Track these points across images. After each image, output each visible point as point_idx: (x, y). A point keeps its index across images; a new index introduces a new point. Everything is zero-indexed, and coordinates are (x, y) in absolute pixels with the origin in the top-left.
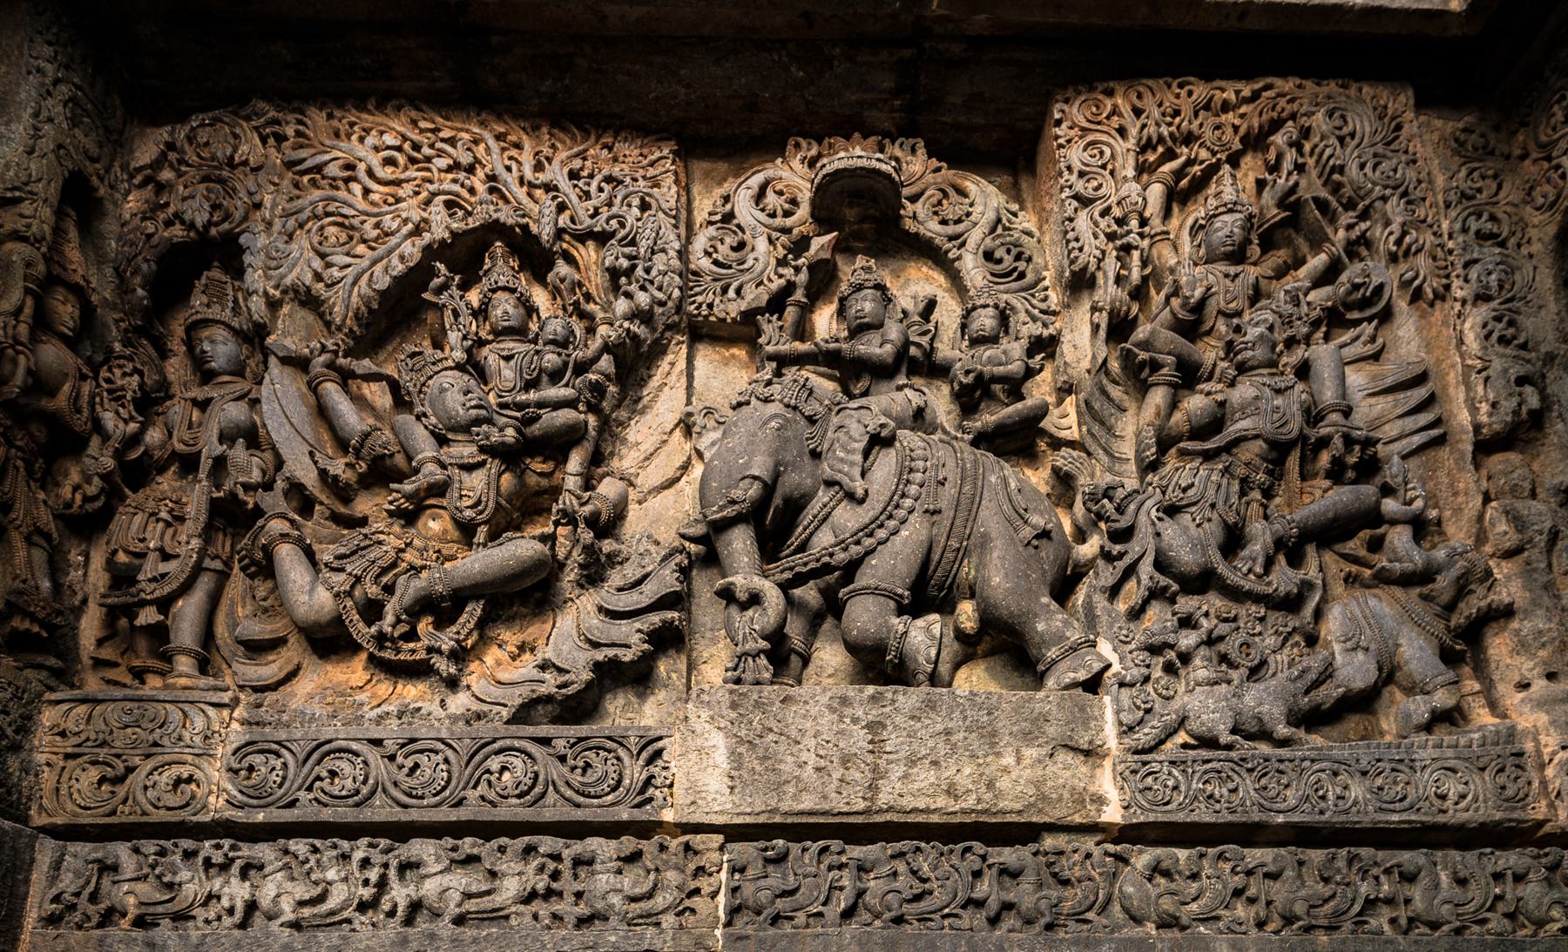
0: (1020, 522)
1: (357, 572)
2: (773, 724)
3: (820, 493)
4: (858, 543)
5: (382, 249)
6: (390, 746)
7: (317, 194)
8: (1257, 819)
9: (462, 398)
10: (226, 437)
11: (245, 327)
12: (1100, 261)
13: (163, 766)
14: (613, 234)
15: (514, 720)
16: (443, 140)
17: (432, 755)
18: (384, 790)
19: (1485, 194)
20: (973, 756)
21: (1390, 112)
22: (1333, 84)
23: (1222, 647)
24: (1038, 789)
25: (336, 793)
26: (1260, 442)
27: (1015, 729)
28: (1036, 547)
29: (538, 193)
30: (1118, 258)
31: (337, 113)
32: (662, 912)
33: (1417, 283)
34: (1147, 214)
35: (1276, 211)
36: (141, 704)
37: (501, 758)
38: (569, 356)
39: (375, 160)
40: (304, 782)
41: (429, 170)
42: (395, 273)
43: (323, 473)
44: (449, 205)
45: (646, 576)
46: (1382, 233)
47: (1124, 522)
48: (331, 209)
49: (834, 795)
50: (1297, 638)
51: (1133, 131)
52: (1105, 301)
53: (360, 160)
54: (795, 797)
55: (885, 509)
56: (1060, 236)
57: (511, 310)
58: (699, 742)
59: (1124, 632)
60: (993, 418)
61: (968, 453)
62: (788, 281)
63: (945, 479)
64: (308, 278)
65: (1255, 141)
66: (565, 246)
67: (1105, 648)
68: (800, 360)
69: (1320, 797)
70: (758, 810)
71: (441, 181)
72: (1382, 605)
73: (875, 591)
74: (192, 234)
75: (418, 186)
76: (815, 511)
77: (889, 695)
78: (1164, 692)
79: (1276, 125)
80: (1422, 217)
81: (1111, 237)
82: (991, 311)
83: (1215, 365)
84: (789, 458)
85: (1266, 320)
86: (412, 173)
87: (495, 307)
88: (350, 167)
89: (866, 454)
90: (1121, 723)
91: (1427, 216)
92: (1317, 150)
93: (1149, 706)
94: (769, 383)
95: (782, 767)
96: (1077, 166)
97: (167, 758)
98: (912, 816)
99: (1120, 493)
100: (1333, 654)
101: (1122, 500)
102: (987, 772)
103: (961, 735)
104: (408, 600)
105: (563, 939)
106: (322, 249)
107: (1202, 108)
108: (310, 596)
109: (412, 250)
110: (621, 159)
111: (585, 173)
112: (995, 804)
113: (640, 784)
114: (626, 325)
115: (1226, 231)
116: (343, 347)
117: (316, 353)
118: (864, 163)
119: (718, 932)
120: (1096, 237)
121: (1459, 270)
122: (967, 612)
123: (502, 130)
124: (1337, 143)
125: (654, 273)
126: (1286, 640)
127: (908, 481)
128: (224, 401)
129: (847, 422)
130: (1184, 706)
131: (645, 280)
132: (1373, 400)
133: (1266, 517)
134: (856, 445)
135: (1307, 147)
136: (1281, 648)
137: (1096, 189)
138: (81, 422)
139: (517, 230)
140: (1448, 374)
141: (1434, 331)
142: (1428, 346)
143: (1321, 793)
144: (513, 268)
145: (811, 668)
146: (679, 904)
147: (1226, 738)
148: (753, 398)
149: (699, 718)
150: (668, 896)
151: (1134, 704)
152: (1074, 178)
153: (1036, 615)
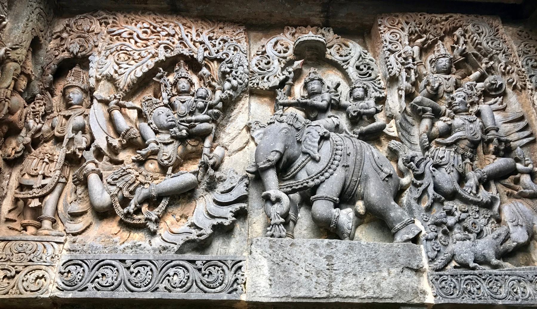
0: (380, 171)
1: (121, 186)
2: (287, 256)
3: (301, 156)
4: (318, 178)
6: (129, 263)
7: (118, 43)
8: (491, 303)
9: (166, 118)
10: (76, 130)
11: (86, 88)
12: (400, 72)
13: (32, 271)
14: (224, 60)
15: (180, 251)
16: (164, 26)
17: (145, 267)
18: (125, 284)
19: (531, 53)
21: (494, 25)
22: (473, 16)
23: (465, 224)
24: (398, 287)
25: (104, 284)
27: (386, 260)
28: (387, 181)
29: (197, 44)
30: (406, 71)
31: (128, 16)
33: (514, 83)
34: (415, 57)
35: (460, 57)
37: (174, 269)
38: (207, 103)
39: (140, 32)
40: (91, 279)
41: (159, 36)
42: (144, 71)
43: (109, 145)
44: (166, 48)
45: (233, 188)
46: (498, 65)
47: (420, 172)
48: (123, 48)
49: (314, 289)
50: (493, 220)
51: (407, 29)
52: (403, 86)
53: (135, 32)
54: (297, 290)
55: (327, 165)
56: (384, 63)
57: (185, 85)
58: (257, 263)
59: (425, 217)
61: (359, 142)
62: (287, 77)
63: (350, 153)
64: (112, 73)
65: (450, 33)
66: (206, 62)
67: (418, 223)
68: (290, 105)
69: (515, 292)
70: (281, 296)
71: (163, 39)
72: (523, 206)
73: (326, 198)
74: (72, 55)
75: (155, 41)
76: (299, 164)
77: (334, 244)
78: (444, 243)
79: (456, 29)
80: (512, 60)
81: (403, 64)
82: (361, 89)
83: (445, 111)
84: (289, 143)
85: (462, 96)
86: (153, 36)
87: (179, 84)
88: (131, 34)
89: (319, 143)
90: (429, 257)
91: (513, 60)
92: (471, 37)
93: (439, 249)
94: (282, 115)
95: (291, 275)
96: (388, 40)
97: (35, 267)
98: (347, 299)
99: (417, 159)
100: (508, 227)
101: (418, 162)
102: (377, 279)
103: (365, 262)
104: (140, 198)
106: (118, 62)
107: (429, 22)
108: (102, 196)
109: (151, 63)
110: (226, 33)
111: (214, 38)
112: (381, 294)
113: (232, 282)
114: (228, 92)
115: (443, 63)
116: (122, 96)
117: (112, 99)
120: (397, 64)
121: (528, 79)
122: (360, 206)
123: (185, 22)
124: (478, 35)
125: (239, 73)
126: (488, 221)
127: (336, 154)
128: (76, 116)
129: (311, 131)
130: (453, 250)
131: (235, 76)
132: (506, 125)
133: (473, 170)
135: (467, 36)
136: (487, 224)
137: (396, 48)
138: (20, 124)
140: (532, 116)
141: (523, 101)
142: (522, 106)
143: (515, 290)
144: (186, 69)
145: (297, 225)
147: (472, 265)
148: (276, 121)
151: (433, 248)
152: (387, 44)
153: (390, 210)
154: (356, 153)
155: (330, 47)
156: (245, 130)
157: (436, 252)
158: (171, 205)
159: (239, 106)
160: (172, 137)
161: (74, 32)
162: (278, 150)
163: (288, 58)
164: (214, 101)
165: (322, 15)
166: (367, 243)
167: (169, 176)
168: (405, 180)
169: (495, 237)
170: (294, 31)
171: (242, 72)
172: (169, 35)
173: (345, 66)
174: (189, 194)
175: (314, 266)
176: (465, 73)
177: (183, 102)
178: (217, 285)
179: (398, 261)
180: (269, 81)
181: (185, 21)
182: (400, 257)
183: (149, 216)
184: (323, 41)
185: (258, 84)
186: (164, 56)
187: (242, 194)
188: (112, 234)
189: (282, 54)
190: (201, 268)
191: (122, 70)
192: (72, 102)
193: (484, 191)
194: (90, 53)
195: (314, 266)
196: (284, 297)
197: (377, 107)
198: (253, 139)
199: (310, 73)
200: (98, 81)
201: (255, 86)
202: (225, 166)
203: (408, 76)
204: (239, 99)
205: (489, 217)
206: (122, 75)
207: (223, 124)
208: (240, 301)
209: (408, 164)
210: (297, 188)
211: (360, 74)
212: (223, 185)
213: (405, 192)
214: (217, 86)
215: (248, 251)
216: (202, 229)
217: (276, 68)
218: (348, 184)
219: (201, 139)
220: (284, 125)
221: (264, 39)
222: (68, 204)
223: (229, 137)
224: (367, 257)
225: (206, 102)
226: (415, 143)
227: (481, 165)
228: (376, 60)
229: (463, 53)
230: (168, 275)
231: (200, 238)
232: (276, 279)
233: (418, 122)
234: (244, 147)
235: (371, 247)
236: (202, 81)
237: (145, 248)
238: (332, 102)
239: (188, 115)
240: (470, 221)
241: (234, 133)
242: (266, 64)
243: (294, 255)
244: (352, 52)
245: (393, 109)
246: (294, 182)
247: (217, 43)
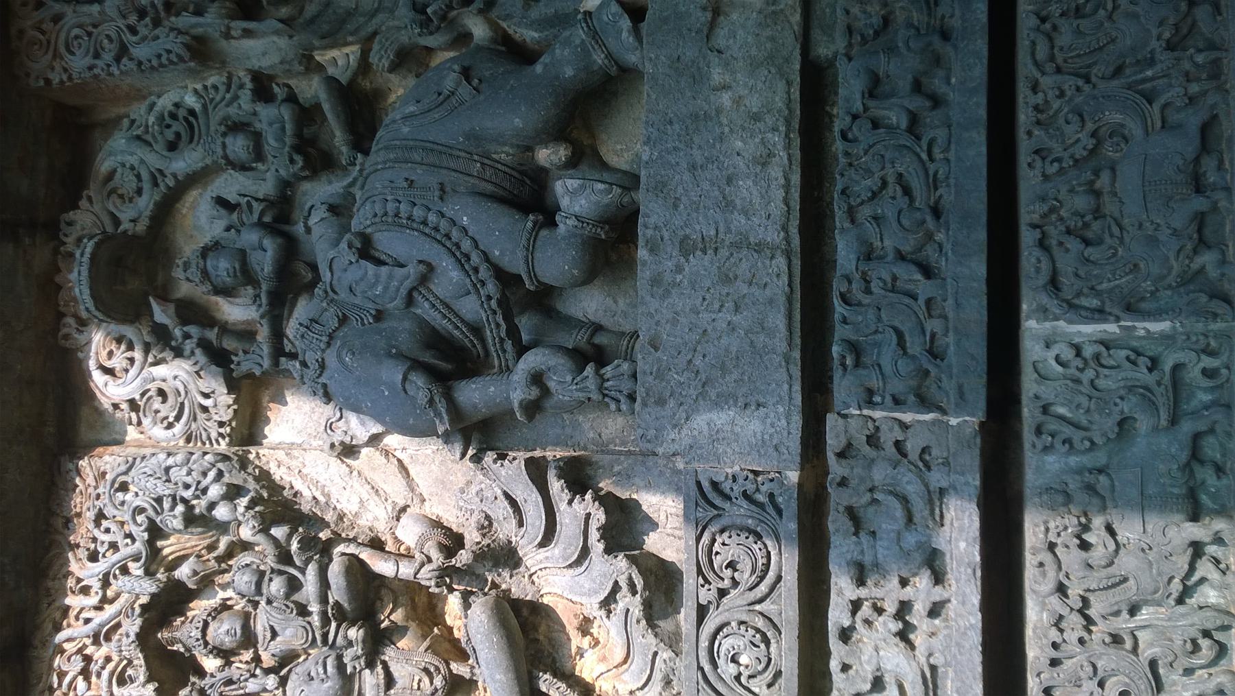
2: (682, 360)
3: (419, 311)
4: (476, 270)
9: (315, 683)
14: (151, 521)
15: (673, 642)
16: (60, 685)
20: (721, 138)
29: (110, 593)
30: (178, 15)
32: (926, 486)
38: (273, 571)
45: (507, 496)
49: (768, 292)
54: (771, 334)
55: (439, 242)
57: (225, 627)
60: (338, 133)
61: (378, 155)
62: (199, 345)
63: (407, 179)
70: (785, 377)
73: (530, 250)
76: (439, 316)
77: (649, 232)
81: (157, 23)
82: (229, 140)
89: (379, 262)
94: (304, 364)
96: (88, 60)
98: (792, 204)
102: (740, 122)
103: (696, 152)
105: (963, 603)
111: (92, 546)
112: (779, 111)
113: (753, 507)
114: (241, 509)
118: (85, 273)
119: (954, 421)
120: (157, 38)
122: (546, 155)
125: (189, 480)
127: (409, 218)
131: (197, 489)
134: (370, 273)
139: (146, 616)
144: (183, 623)
145: (606, 322)
146: (916, 467)
148: (320, 381)
149: (675, 439)
150: (905, 479)
152: (99, 63)
153: (557, 78)
155: (116, 222)
158: (554, 661)
159: (287, 478)
160: (370, 665)
163: (148, 339)
164: (270, 550)
165: (27, 241)
166: (645, 143)
167: (477, 671)
168: (479, 30)
170: (70, 320)
172: (85, 673)
173: (166, 180)
174: (525, 612)
175: (709, 288)
177: (274, 634)
178: (762, 547)
179: (693, 62)
180: (213, 392)
181: (49, 626)
182: (683, 57)
184: (91, 244)
185: (221, 424)
186: (144, 686)
187: (524, 472)
190: (718, 589)
195: (709, 288)
196: (788, 370)
197: (280, 98)
199: (188, 279)
202: (452, 519)
204: (264, 477)
207: (335, 518)
208: (799, 484)
209: (432, 21)
210: (504, 327)
211: (191, 141)
212: (499, 522)
213: (511, 32)
216: (616, 583)
217: (176, 373)
219: (377, 583)
220: (331, 359)
223: (371, 502)
224: (682, 146)
225: (271, 573)
228: (150, 94)
230: (738, 678)
231: (639, 587)
232: (744, 390)
234: (399, 461)
235: (656, 133)
238: (267, 219)
239: (307, 619)
241: (361, 489)
242: (164, 401)
243: (680, 341)
244: (132, 160)
245: (283, 54)
246: (488, 333)
247: (106, 538)
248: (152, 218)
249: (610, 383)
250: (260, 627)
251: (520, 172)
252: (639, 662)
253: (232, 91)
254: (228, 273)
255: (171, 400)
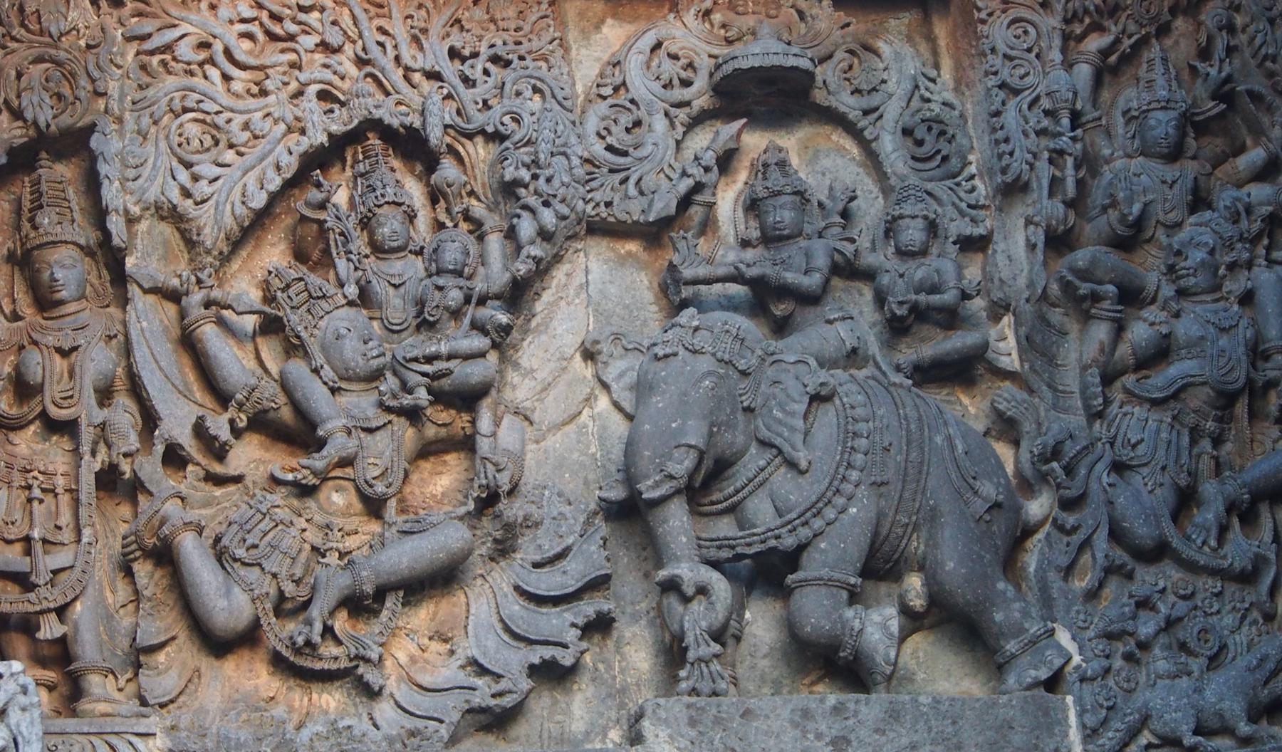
3: (753, 450)
4: (805, 524)
5: (252, 155)
7: (171, 82)
9: (363, 348)
26: (1207, 389)
27: (980, 739)
29: (417, 77)
30: (1051, 161)
34: (1079, 106)
36: (65, 738)
44: (324, 96)
51: (1059, 7)
59: (1082, 617)
64: (175, 195)
67: (1064, 637)
73: (828, 583)
74: (32, 132)
75: (284, 73)
77: (851, 706)
82: (920, 223)
85: (1206, 243)
87: (381, 225)
89: (805, 417)
99: (1070, 450)
101: (1072, 458)
115: (1160, 131)
120: (1025, 134)
125: (556, 183)
127: (852, 448)
129: (783, 377)
130: (1146, 705)
131: (549, 195)
137: (1022, 78)
139: (401, 130)
145: (744, 645)
151: (1096, 701)
152: (997, 61)
153: (993, 605)
154: (909, 443)
156: (578, 357)
157: (1104, 712)
159: (555, 282)
161: (18, 41)
162: (693, 443)
168: (1037, 507)
169: (1252, 666)
171: (566, 179)
172: (324, 46)
176: (1223, 152)
177: (396, 286)
182: (1013, 732)
183: (361, 650)
186: (325, 130)
187: (598, 573)
188: (263, 700)
189: (679, 94)
191: (203, 188)
192: (64, 294)
193: (1240, 537)
194: (87, 120)
198: (605, 386)
200: (131, 221)
201: (602, 210)
203: (1058, 174)
204: (557, 259)
205: (1247, 610)
206: (206, 206)
207: (514, 342)
211: (913, 158)
214: (492, 221)
215: (621, 728)
218: (884, 531)
221: (609, 21)
222: (112, 616)
223: (533, 383)
226: (1068, 389)
227: (1241, 456)
229: (1222, 91)
233: (1078, 321)
236: (442, 203)
237: (364, 735)
240: (1195, 625)
242: (628, 130)
248: (828, 108)
249: (705, 670)
250: (396, 266)
251: (897, 561)
252: (423, 703)
253: (969, 210)
254: (779, 222)
255: (628, 139)
